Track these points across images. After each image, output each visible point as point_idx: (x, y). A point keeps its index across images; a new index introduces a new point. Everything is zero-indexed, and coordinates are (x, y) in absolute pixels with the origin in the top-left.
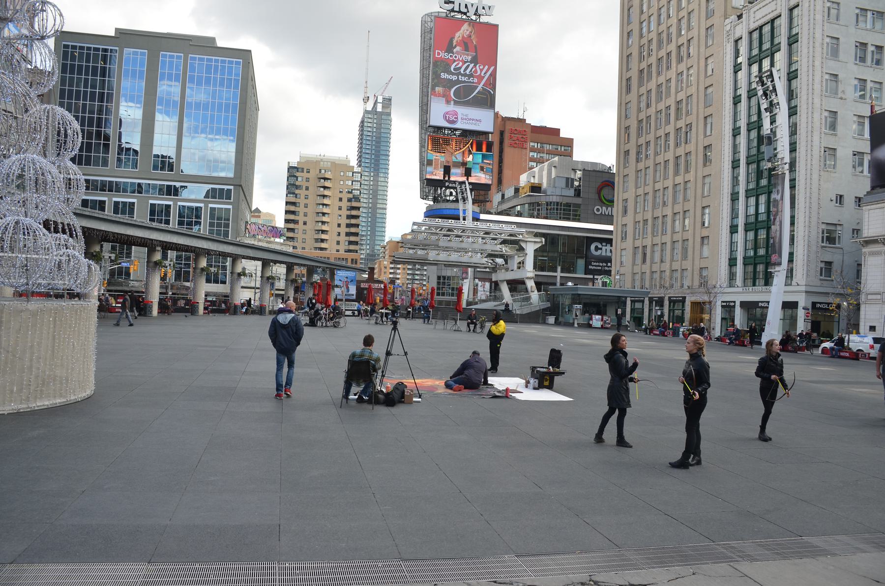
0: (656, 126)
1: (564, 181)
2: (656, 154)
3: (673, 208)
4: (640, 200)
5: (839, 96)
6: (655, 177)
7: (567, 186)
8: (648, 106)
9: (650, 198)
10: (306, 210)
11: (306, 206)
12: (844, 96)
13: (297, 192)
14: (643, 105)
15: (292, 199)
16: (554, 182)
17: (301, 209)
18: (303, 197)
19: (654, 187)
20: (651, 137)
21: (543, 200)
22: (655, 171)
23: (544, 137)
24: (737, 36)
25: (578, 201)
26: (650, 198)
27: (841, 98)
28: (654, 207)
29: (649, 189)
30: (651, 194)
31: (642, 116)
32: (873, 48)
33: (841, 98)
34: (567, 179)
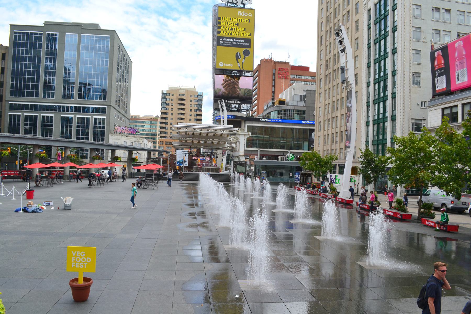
0: (333, 63)
1: (299, 97)
2: (334, 80)
3: (341, 112)
4: (327, 107)
5: (422, 40)
6: (333, 93)
7: (301, 100)
8: (330, 52)
9: (331, 106)
10: (172, 117)
11: (172, 114)
12: (425, 41)
13: (167, 107)
14: (328, 52)
15: (164, 111)
16: (293, 98)
17: (169, 116)
18: (170, 109)
19: (332, 100)
20: (331, 71)
21: (284, 107)
22: (333, 90)
23: (300, 72)
24: (369, 7)
25: (304, 109)
26: (331, 106)
27: (424, 42)
28: (333, 112)
29: (330, 101)
30: (331, 104)
31: (327, 58)
32: (444, 11)
33: (424, 42)
34: (301, 96)
